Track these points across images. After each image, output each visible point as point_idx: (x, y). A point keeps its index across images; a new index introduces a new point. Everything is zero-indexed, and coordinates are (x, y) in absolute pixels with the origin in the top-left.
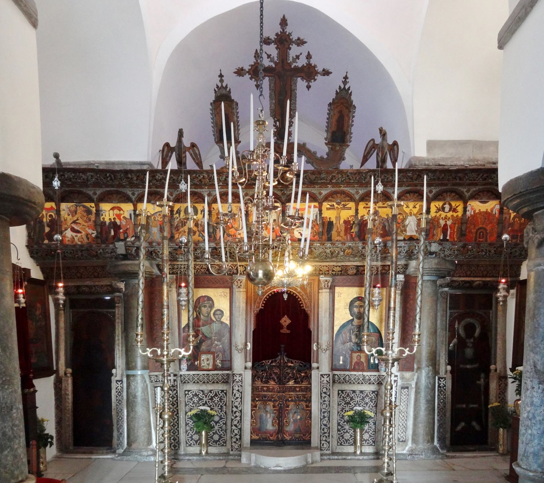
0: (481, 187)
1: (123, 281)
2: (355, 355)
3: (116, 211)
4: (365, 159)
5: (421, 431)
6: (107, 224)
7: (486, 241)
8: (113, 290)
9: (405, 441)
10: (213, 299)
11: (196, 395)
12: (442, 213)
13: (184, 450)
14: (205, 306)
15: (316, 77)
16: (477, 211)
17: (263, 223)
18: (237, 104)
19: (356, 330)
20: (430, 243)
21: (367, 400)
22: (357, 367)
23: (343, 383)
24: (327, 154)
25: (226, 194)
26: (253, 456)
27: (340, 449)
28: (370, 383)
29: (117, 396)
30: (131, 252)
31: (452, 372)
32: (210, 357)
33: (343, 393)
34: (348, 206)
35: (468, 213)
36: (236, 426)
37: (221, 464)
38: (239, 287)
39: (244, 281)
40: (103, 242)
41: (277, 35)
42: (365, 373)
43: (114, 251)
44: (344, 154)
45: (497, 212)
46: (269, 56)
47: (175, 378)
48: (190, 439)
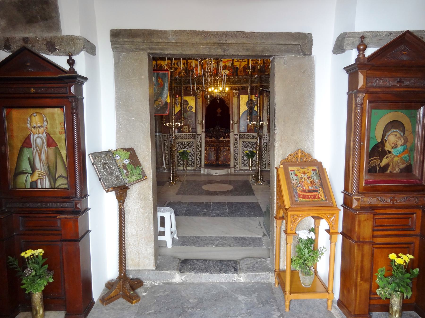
11: (181, 144)
32: (187, 127)
42: (253, 134)
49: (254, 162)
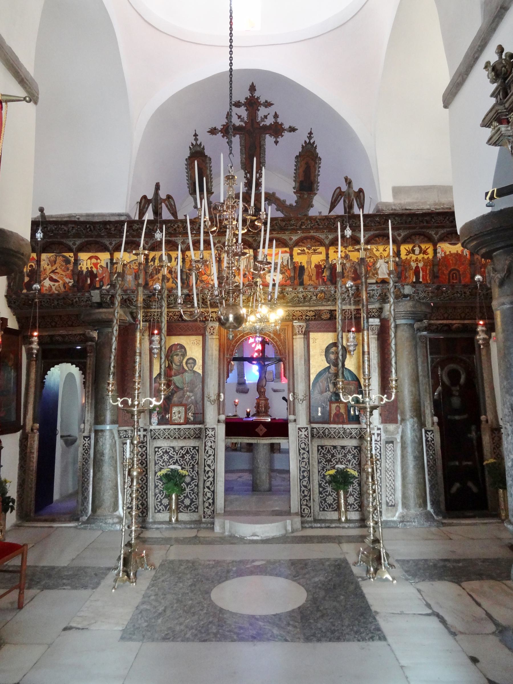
0: (448, 230)
1: (96, 330)
2: (334, 406)
3: (94, 261)
4: (333, 206)
5: (412, 492)
6: (84, 273)
7: (460, 282)
8: (85, 339)
9: (394, 506)
10: (186, 346)
11: (167, 452)
12: (412, 255)
13: (153, 517)
14: (177, 355)
15: (283, 134)
16: (448, 253)
17: (234, 268)
18: (210, 159)
19: (333, 378)
20: (403, 286)
21: (350, 457)
22: (336, 419)
23: (323, 437)
24: (296, 202)
25: (199, 241)
26: (227, 523)
27: (322, 516)
28: (351, 438)
29: (83, 455)
30: (106, 299)
31: (439, 424)
32: (182, 409)
33: (323, 449)
34: (318, 251)
35: (439, 255)
36: (208, 488)
37: (192, 533)
38: (212, 334)
39: (217, 328)
40: (79, 290)
41: (246, 98)
42: (345, 426)
43: (89, 299)
44: (312, 202)
45: (468, 253)
46: (239, 117)
47: (145, 433)
48: (159, 504)
49: (351, 500)
